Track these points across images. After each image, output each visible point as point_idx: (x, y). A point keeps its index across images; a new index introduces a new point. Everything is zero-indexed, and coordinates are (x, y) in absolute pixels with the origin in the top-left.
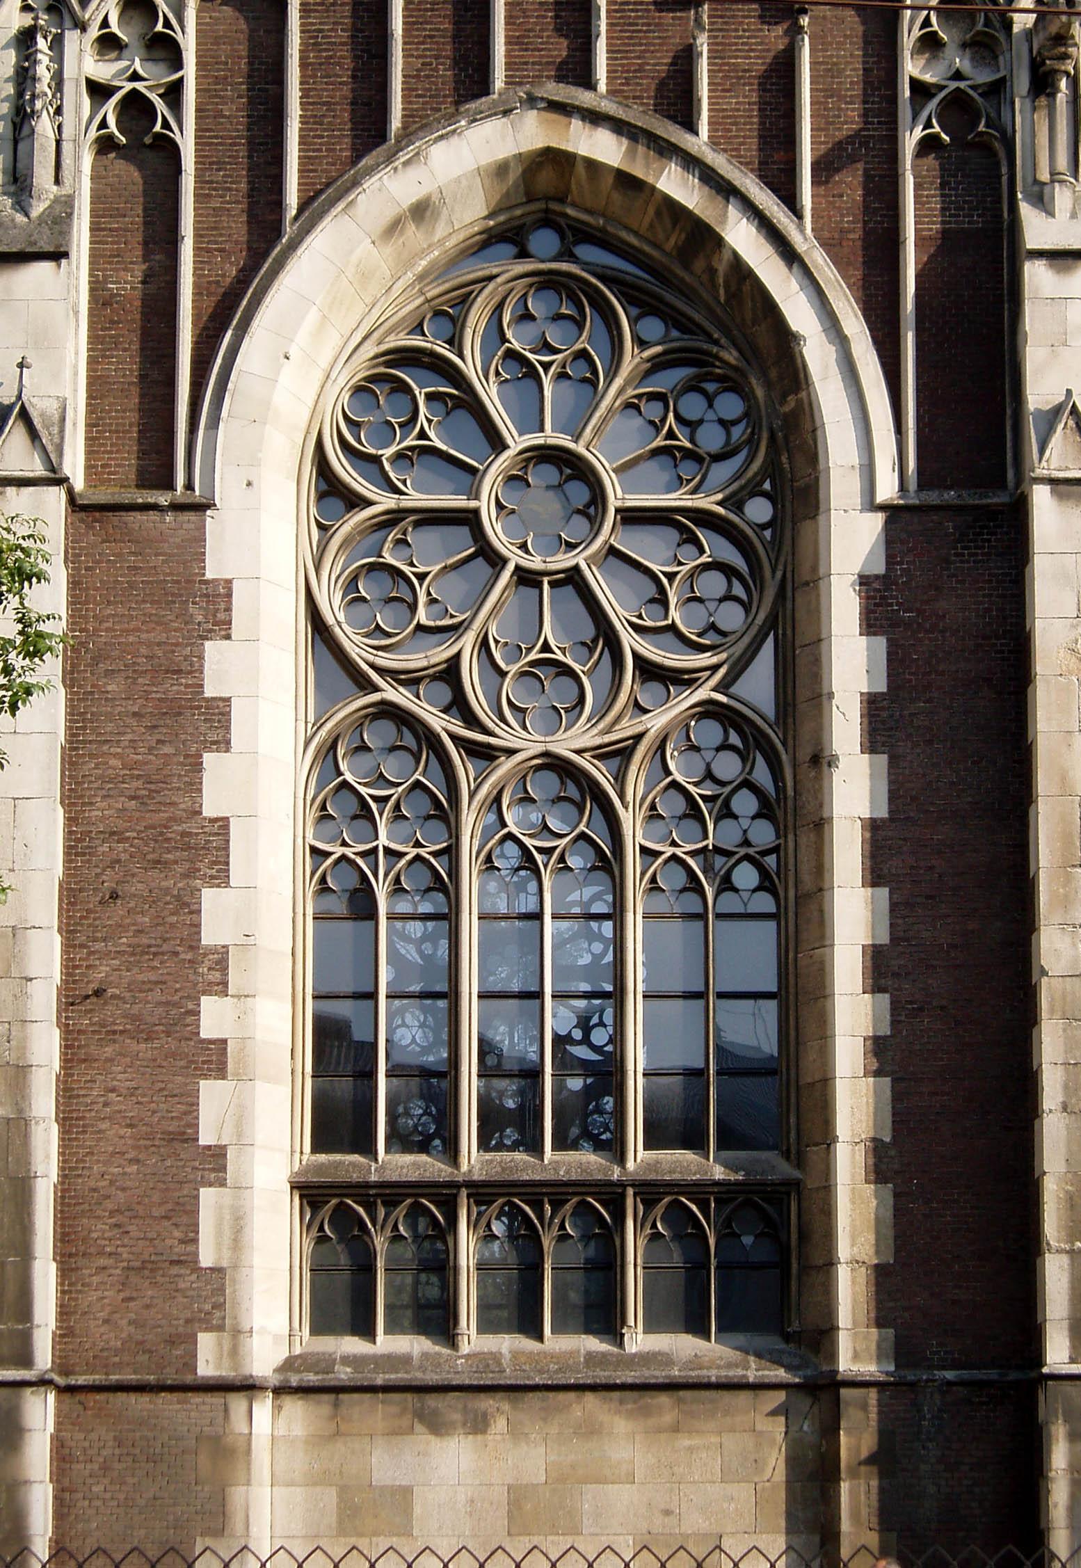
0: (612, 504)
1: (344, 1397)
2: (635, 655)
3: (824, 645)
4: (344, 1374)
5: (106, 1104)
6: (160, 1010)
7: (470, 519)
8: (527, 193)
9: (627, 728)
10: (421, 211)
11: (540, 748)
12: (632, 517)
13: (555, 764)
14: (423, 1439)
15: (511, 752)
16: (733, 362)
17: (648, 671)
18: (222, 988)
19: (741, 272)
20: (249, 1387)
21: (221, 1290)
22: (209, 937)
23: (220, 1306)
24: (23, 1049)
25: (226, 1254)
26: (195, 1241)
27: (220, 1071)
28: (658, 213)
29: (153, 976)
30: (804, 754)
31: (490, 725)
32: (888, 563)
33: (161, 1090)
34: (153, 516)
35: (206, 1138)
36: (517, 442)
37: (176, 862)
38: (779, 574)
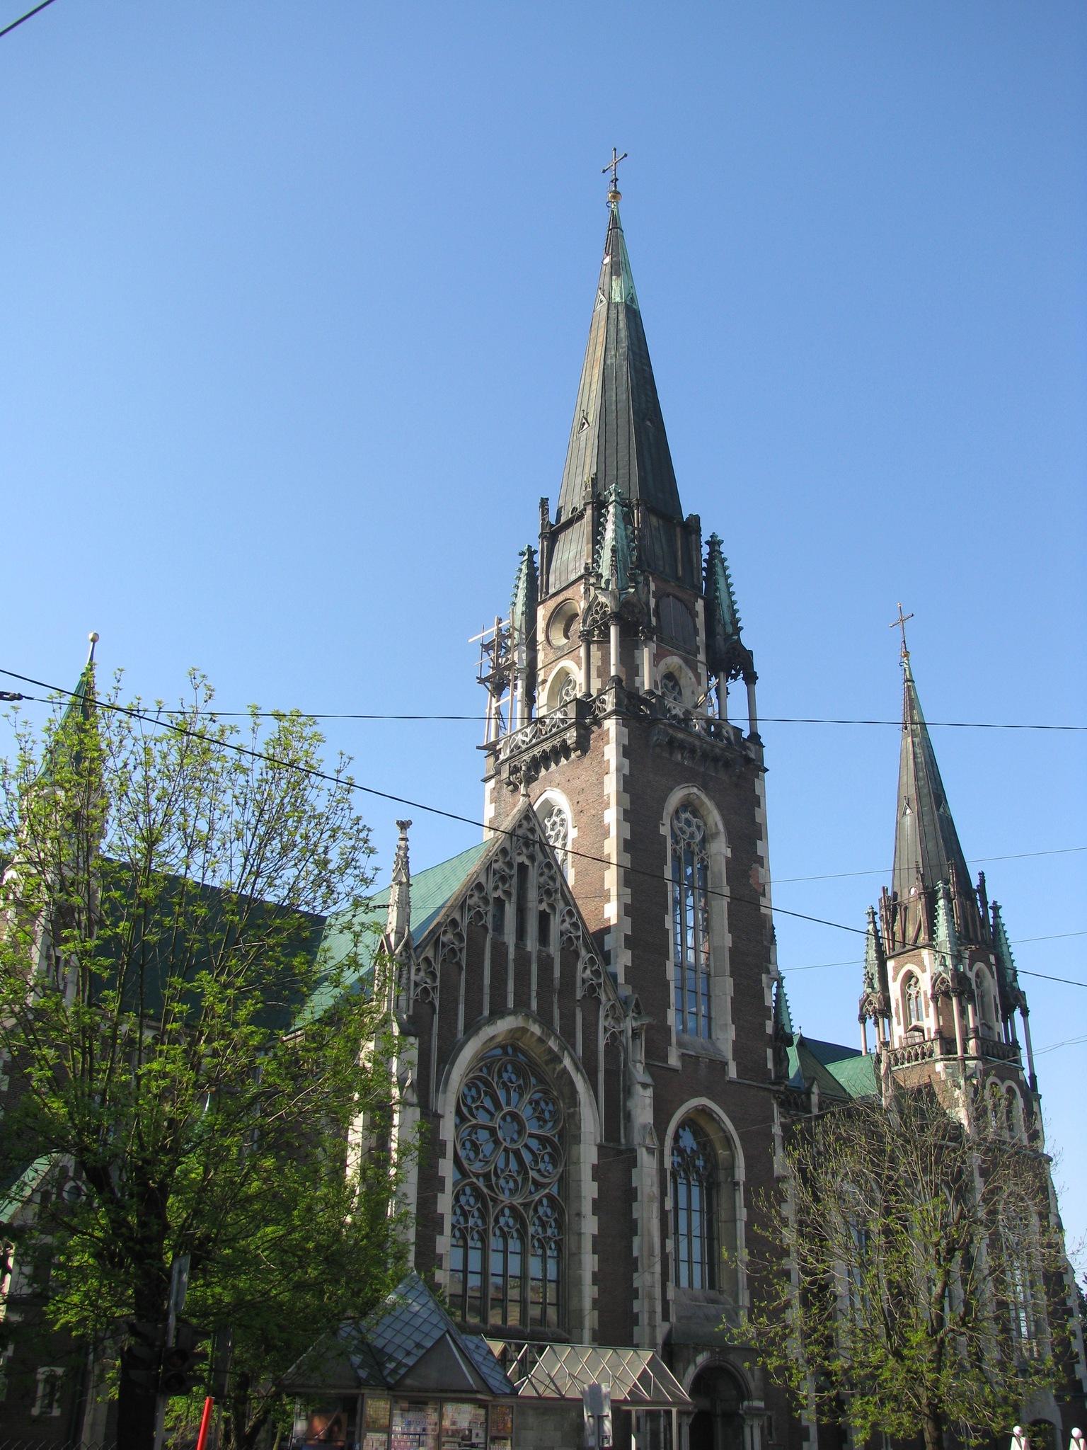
10: (493, 1038)
13: (513, 1208)
17: (535, 1182)
18: (440, 1267)
19: (565, 1070)
22: (438, 1251)
36: (506, 1109)
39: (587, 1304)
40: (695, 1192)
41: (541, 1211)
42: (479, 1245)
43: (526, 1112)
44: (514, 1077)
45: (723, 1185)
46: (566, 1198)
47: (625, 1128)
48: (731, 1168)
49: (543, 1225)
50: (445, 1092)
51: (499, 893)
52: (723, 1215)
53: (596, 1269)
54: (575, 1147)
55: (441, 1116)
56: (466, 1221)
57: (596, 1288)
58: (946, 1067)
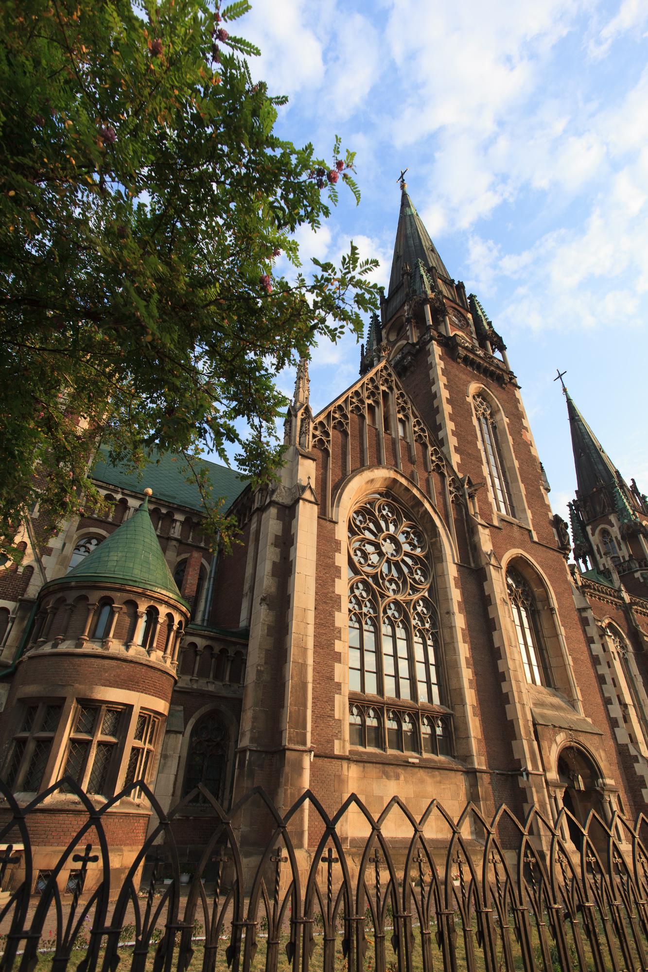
1: (366, 765)
3: (448, 589)
4: (365, 757)
6: (325, 642)
9: (409, 598)
10: (372, 481)
14: (385, 780)
18: (340, 638)
22: (337, 625)
24: (306, 643)
25: (341, 715)
26: (334, 710)
27: (340, 661)
30: (444, 611)
34: (325, 522)
35: (336, 680)
39: (466, 684)
40: (524, 614)
41: (419, 609)
42: (372, 629)
43: (402, 538)
44: (390, 515)
45: (542, 612)
46: (437, 601)
47: (473, 556)
48: (547, 599)
49: (422, 620)
50: (338, 506)
52: (546, 632)
54: (439, 566)
55: (336, 523)
56: (361, 608)
58: (642, 574)
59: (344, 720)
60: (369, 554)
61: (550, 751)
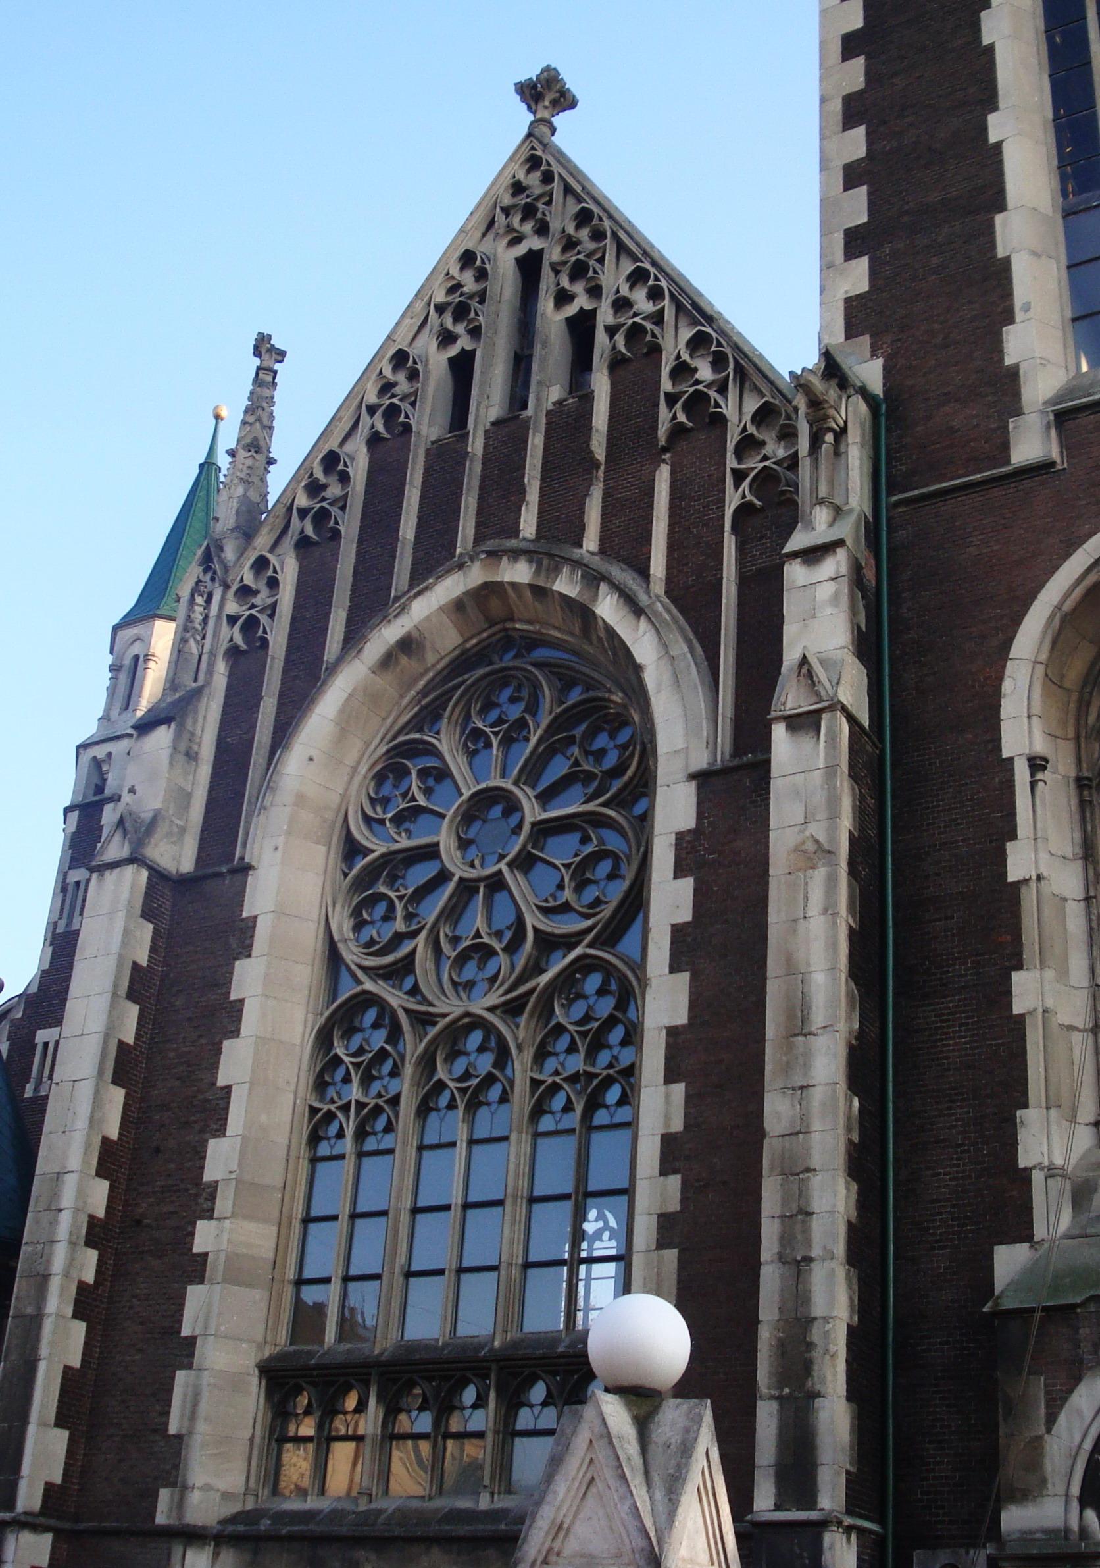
0: (529, 819)
2: (536, 930)
4: (265, 1524)
5: (131, 1308)
7: (431, 852)
8: (487, 619)
10: (407, 645)
11: (458, 1012)
12: (545, 830)
15: (444, 1016)
16: (619, 700)
17: (548, 944)
18: (209, 1214)
20: (193, 1536)
21: (178, 1454)
23: (176, 1467)
25: (186, 1423)
26: (168, 1413)
28: (562, 608)
29: (172, 1209)
31: (430, 997)
32: (698, 818)
33: (165, 1294)
37: (196, 1122)
38: (642, 849)
51: (464, 342)
53: (677, 1125)
57: (675, 1181)
59: (190, 1433)
60: (401, 898)
61: (1051, 1420)
